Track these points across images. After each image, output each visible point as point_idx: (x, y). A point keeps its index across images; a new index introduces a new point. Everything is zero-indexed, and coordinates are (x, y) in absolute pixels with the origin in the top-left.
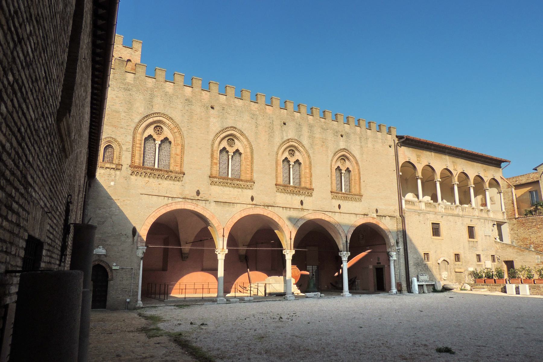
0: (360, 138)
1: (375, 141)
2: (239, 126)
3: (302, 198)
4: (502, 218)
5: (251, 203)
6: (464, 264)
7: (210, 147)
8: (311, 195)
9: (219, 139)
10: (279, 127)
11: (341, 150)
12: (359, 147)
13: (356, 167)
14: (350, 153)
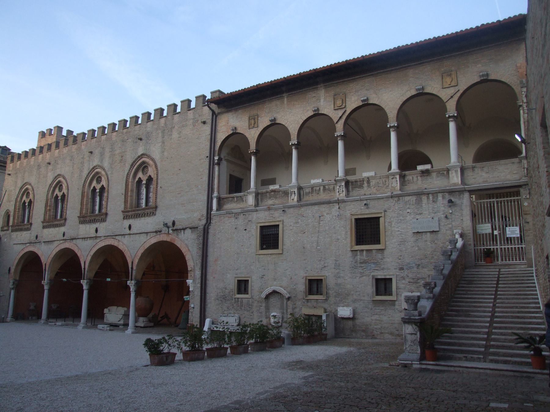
0: (163, 132)
1: (183, 126)
2: (62, 173)
3: (97, 225)
4: (517, 177)
5: (63, 238)
6: (332, 299)
7: (45, 198)
8: (104, 220)
9: (52, 189)
10: (87, 158)
11: (139, 157)
12: (161, 144)
13: (155, 172)
14: (149, 157)
